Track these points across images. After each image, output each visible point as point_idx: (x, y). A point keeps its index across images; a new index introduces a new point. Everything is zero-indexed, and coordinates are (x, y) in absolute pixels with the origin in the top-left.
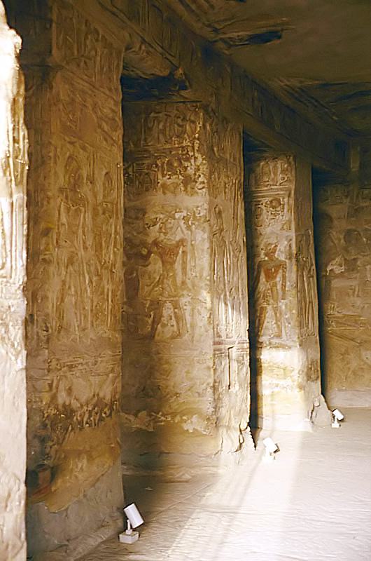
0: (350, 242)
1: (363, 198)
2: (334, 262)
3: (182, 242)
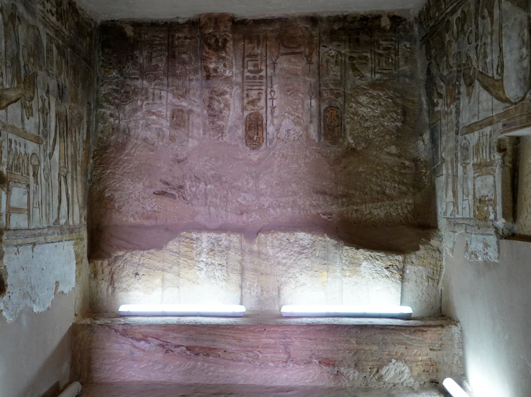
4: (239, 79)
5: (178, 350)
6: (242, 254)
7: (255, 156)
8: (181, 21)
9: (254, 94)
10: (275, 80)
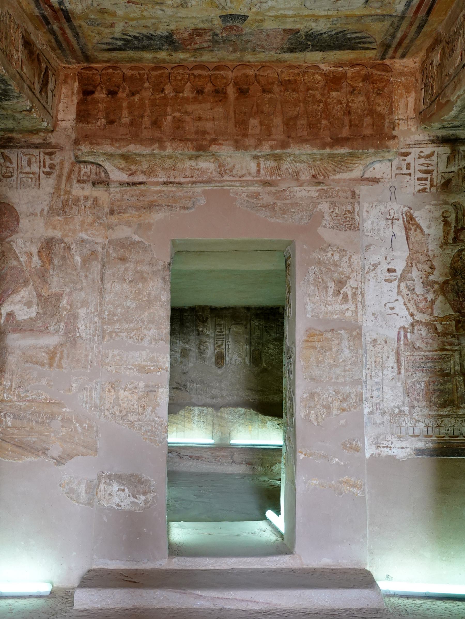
0: (51, 261)
1: (79, 181)
2: (17, 298)
4: (213, 335)
5: (185, 457)
6: (213, 417)
7: (220, 371)
8: (186, 308)
9: (220, 343)
10: (230, 336)
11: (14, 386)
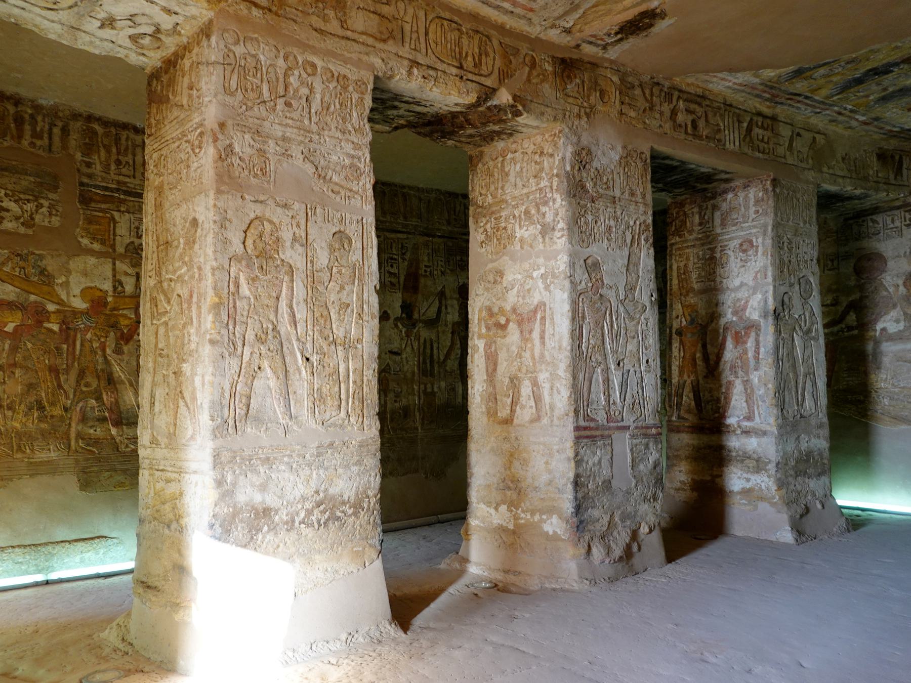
2: (888, 317)
3: (542, 305)
11: (889, 377)
